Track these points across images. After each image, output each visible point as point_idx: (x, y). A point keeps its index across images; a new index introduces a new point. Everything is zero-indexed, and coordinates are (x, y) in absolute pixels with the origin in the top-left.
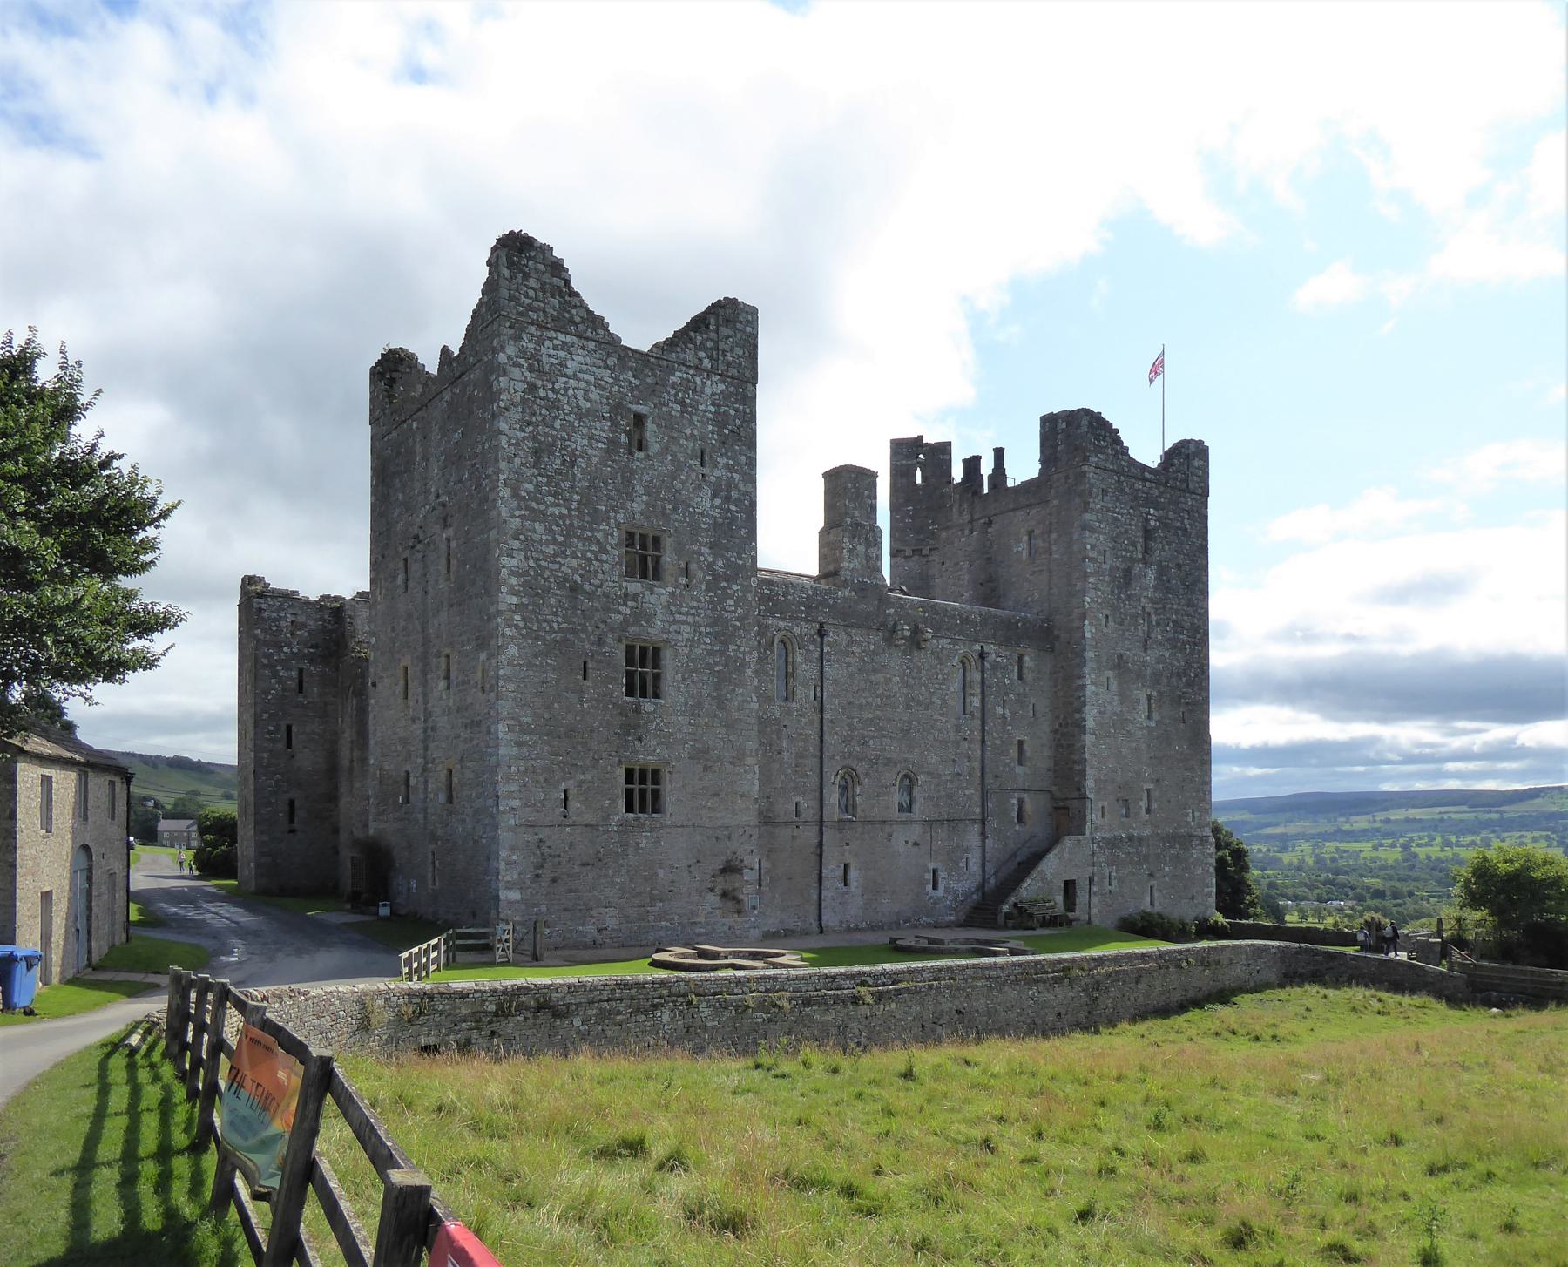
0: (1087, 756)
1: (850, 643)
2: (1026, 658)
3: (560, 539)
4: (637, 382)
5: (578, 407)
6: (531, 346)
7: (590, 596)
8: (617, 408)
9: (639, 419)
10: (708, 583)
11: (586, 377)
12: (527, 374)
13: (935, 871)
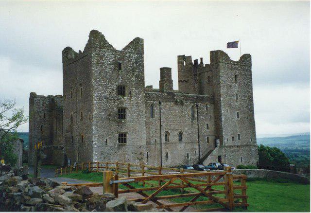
9: (120, 64)
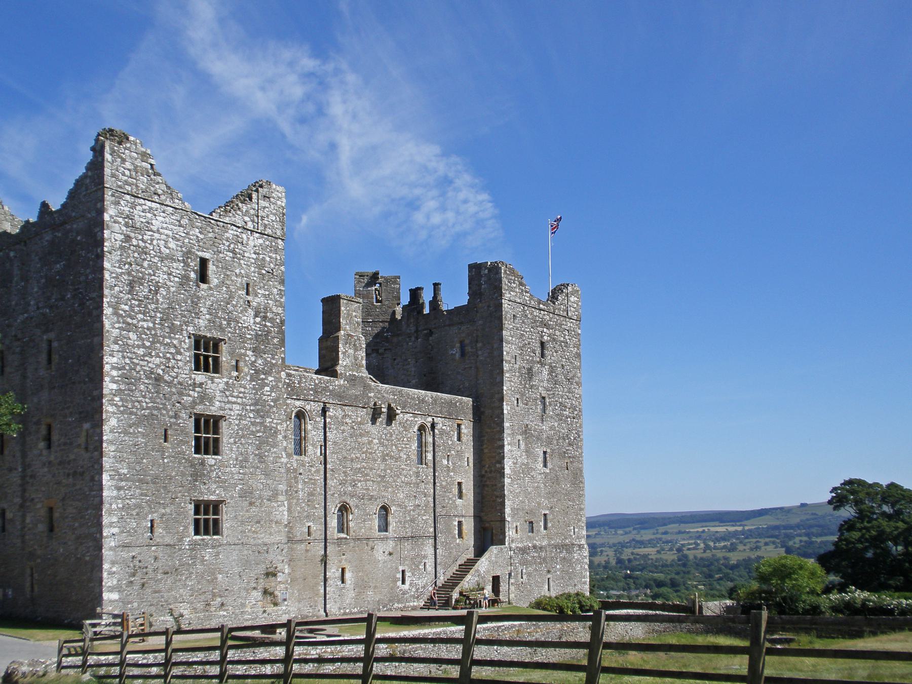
0: (506, 492)
1: (345, 416)
2: (463, 427)
3: (148, 344)
4: (201, 236)
5: (160, 252)
6: (127, 209)
7: (170, 384)
8: (188, 254)
9: (204, 262)
10: (252, 375)
11: (166, 232)
12: (124, 228)
13: (403, 572)
